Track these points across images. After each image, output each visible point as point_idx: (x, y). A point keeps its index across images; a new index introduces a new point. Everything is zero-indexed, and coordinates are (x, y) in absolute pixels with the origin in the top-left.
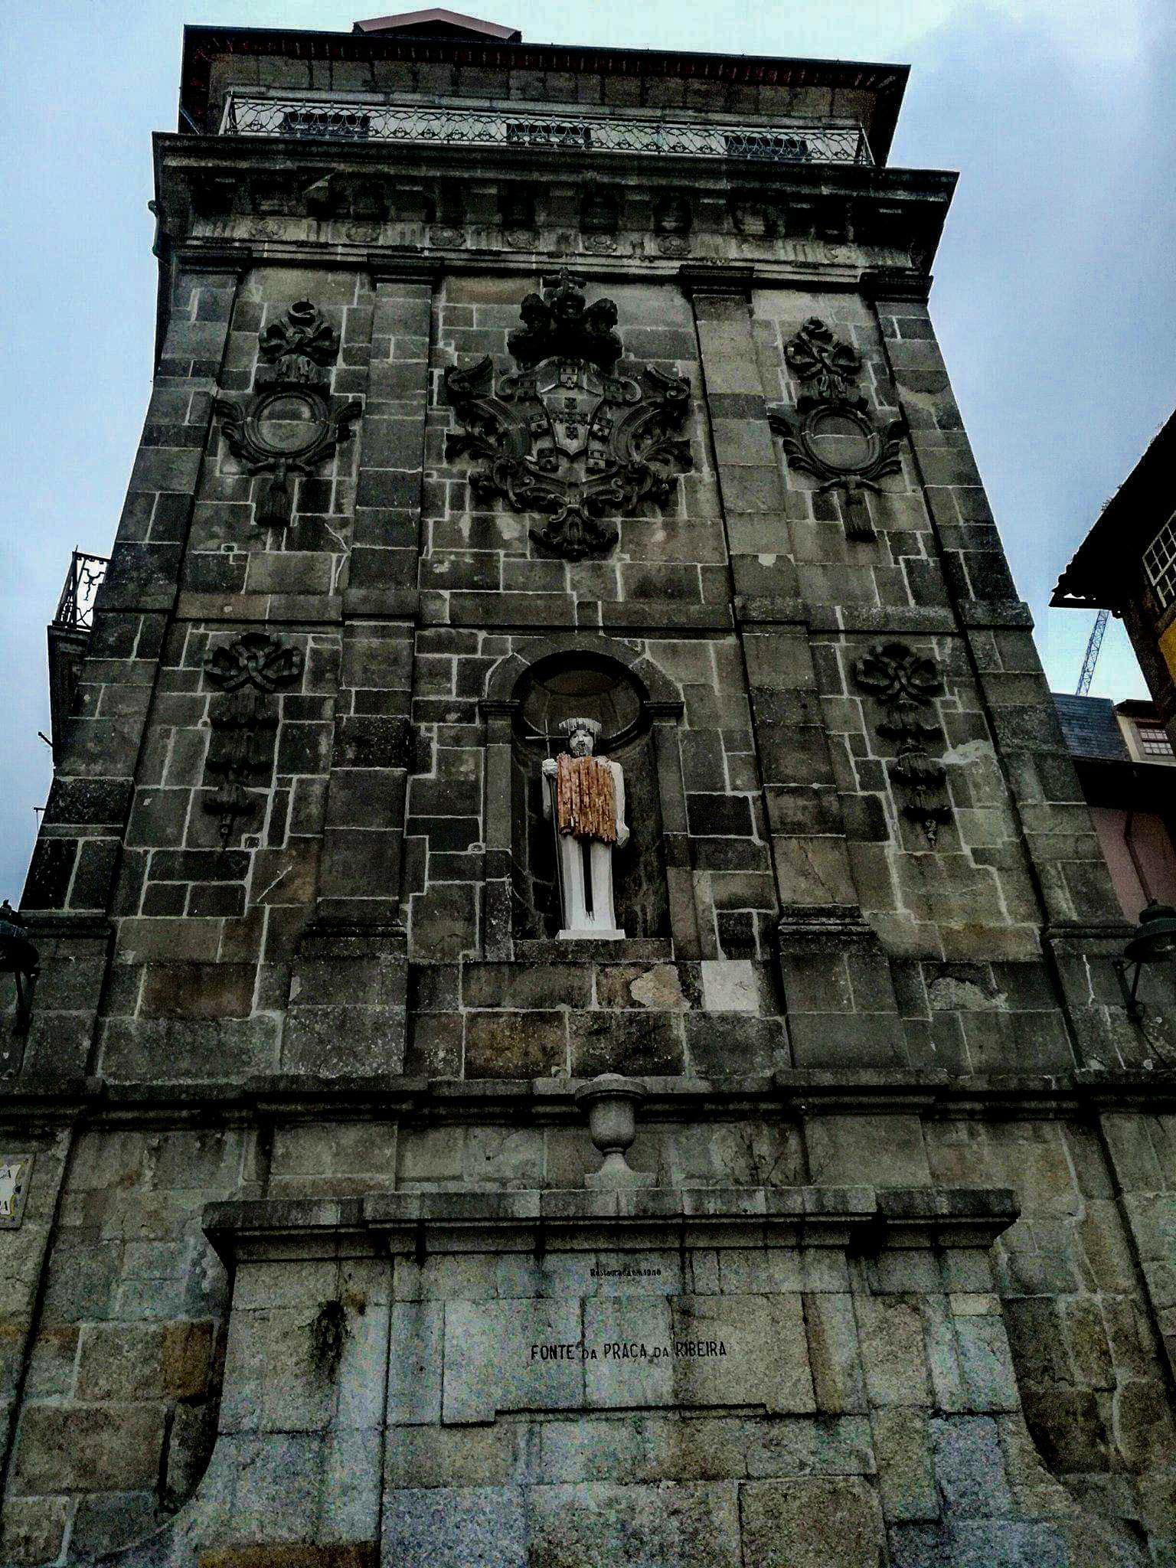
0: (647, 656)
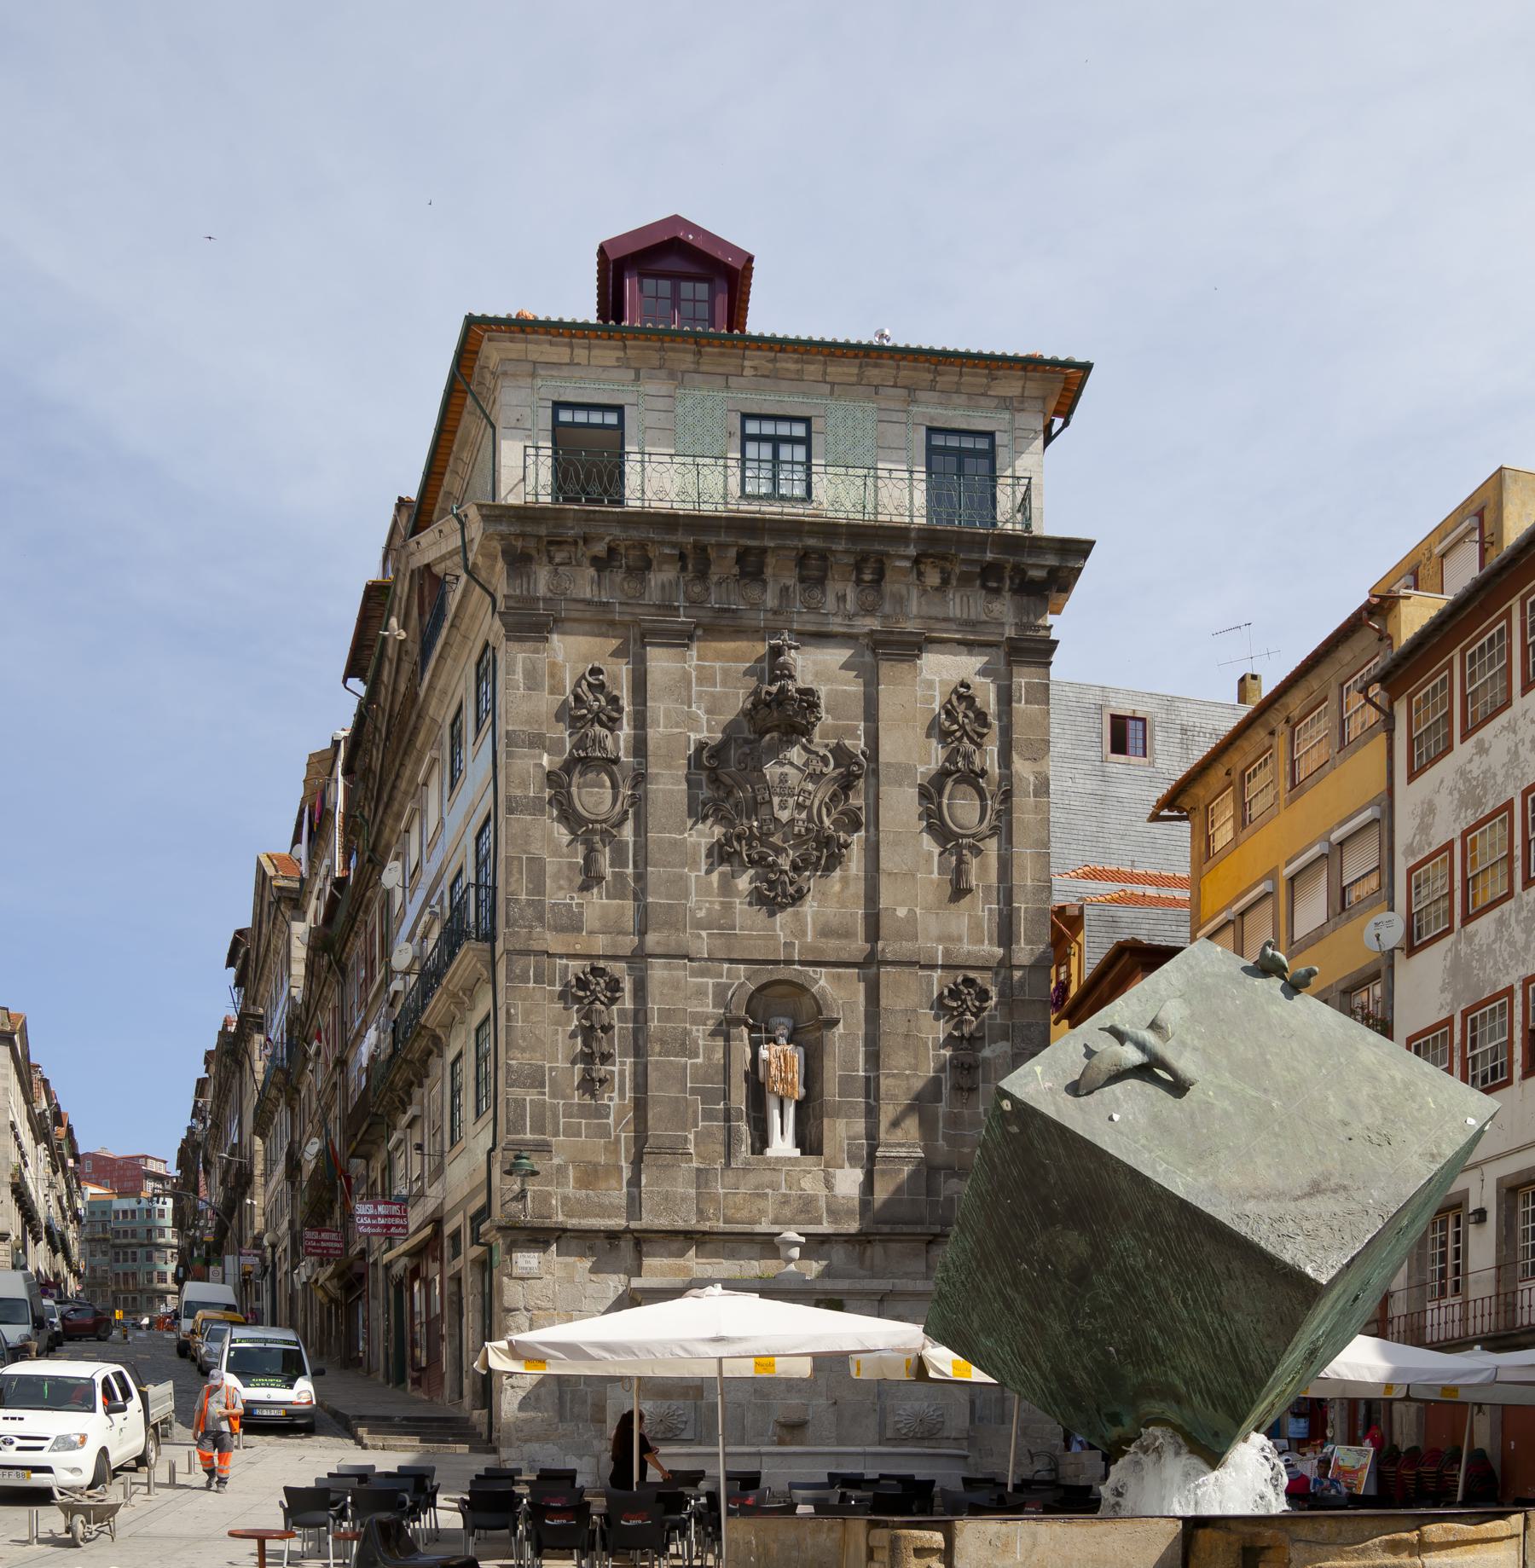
0: (822, 982)
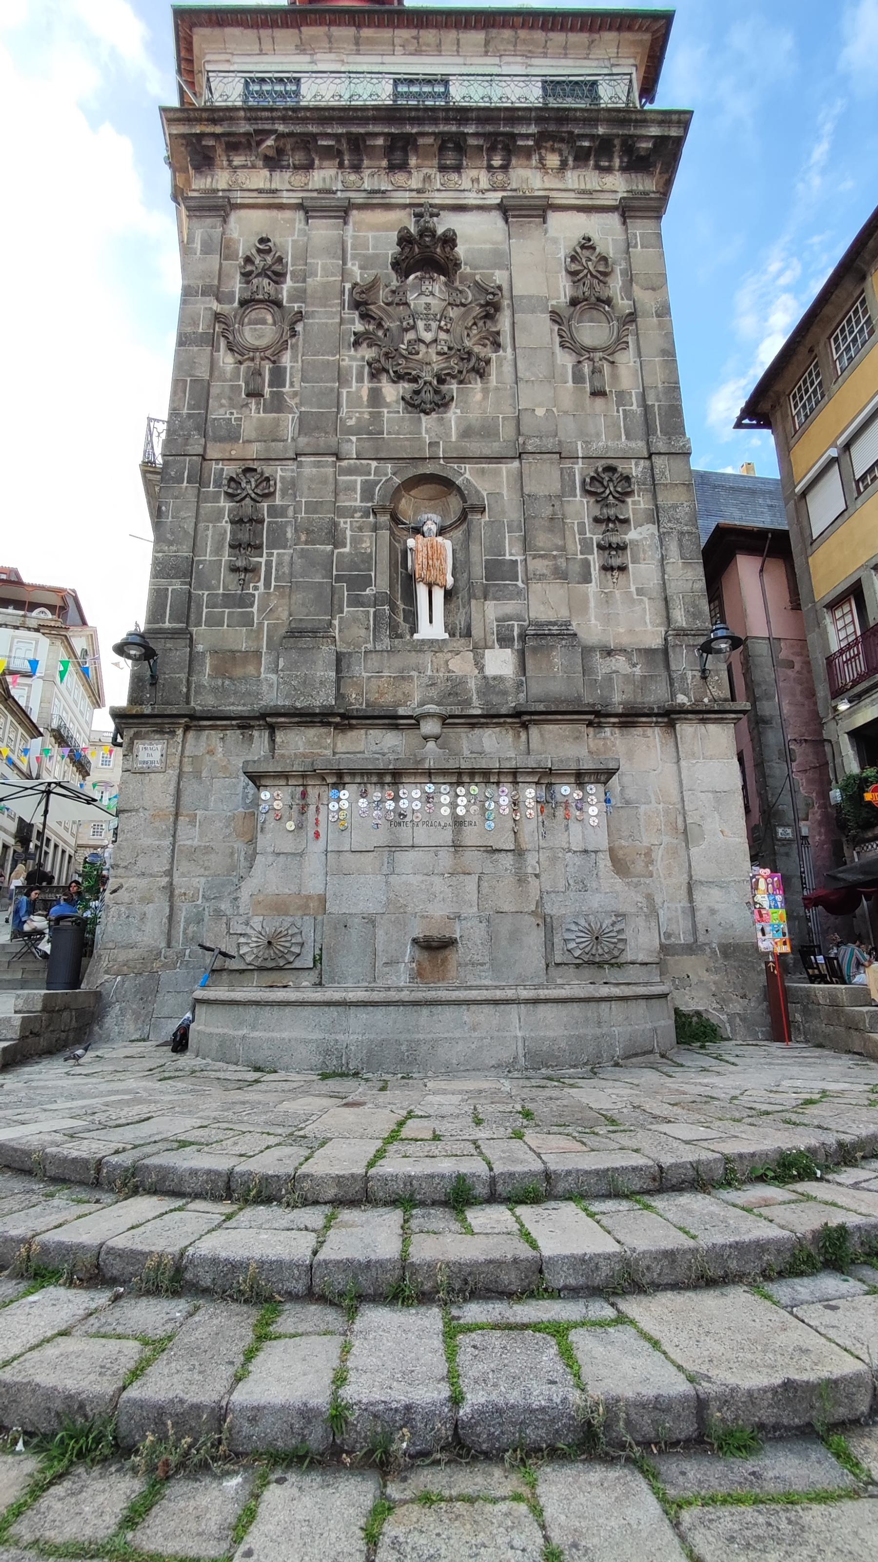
0: (467, 475)
